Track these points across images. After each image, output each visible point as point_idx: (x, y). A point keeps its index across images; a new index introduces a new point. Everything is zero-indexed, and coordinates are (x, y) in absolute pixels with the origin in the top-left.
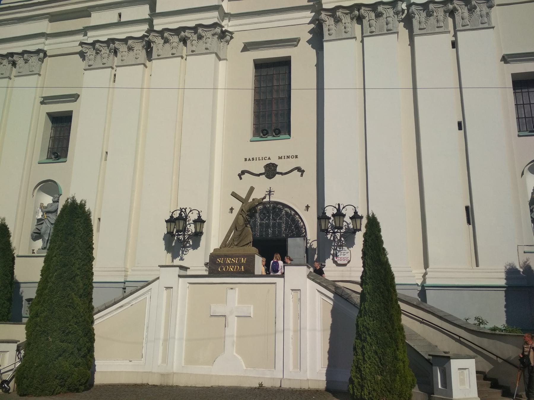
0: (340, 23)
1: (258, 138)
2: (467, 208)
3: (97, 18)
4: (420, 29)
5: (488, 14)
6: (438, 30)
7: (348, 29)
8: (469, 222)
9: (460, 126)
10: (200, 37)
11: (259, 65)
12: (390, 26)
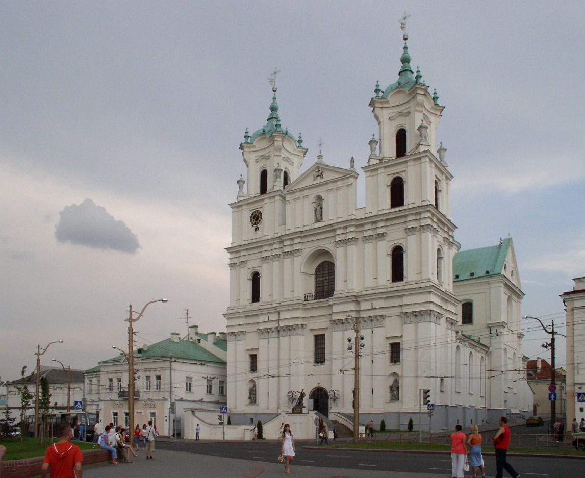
1: (316, 364)
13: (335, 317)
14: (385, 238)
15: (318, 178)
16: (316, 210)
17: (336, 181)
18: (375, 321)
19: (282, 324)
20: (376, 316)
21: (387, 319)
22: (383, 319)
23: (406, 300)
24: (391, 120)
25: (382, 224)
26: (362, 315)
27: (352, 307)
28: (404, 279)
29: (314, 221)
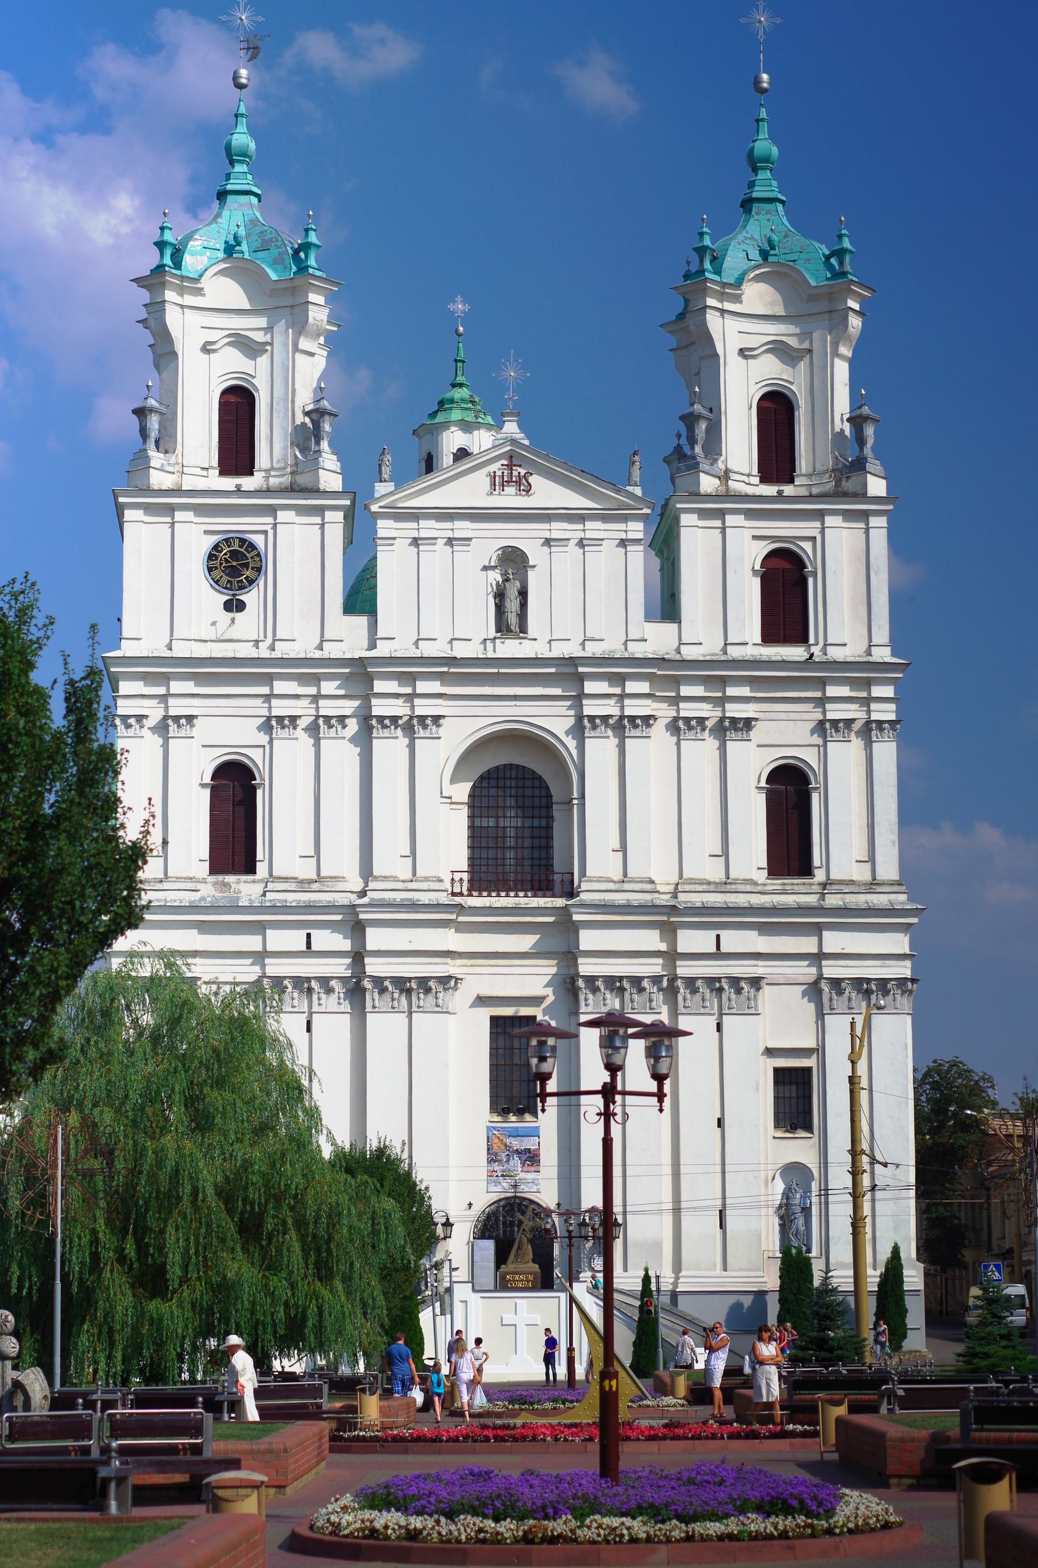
2: (721, 1211)
3: (279, 940)
4: (685, 1007)
6: (702, 1011)
8: (721, 1227)
9: (720, 1123)
10: (428, 990)
12: (654, 1004)
13: (587, 967)
14: (752, 734)
15: (511, 490)
16: (500, 596)
19: (374, 967)
21: (767, 990)
22: (758, 989)
23: (834, 941)
24: (746, 357)
25: (745, 691)
26: (685, 969)
27: (651, 940)
28: (816, 872)
29: (492, 633)
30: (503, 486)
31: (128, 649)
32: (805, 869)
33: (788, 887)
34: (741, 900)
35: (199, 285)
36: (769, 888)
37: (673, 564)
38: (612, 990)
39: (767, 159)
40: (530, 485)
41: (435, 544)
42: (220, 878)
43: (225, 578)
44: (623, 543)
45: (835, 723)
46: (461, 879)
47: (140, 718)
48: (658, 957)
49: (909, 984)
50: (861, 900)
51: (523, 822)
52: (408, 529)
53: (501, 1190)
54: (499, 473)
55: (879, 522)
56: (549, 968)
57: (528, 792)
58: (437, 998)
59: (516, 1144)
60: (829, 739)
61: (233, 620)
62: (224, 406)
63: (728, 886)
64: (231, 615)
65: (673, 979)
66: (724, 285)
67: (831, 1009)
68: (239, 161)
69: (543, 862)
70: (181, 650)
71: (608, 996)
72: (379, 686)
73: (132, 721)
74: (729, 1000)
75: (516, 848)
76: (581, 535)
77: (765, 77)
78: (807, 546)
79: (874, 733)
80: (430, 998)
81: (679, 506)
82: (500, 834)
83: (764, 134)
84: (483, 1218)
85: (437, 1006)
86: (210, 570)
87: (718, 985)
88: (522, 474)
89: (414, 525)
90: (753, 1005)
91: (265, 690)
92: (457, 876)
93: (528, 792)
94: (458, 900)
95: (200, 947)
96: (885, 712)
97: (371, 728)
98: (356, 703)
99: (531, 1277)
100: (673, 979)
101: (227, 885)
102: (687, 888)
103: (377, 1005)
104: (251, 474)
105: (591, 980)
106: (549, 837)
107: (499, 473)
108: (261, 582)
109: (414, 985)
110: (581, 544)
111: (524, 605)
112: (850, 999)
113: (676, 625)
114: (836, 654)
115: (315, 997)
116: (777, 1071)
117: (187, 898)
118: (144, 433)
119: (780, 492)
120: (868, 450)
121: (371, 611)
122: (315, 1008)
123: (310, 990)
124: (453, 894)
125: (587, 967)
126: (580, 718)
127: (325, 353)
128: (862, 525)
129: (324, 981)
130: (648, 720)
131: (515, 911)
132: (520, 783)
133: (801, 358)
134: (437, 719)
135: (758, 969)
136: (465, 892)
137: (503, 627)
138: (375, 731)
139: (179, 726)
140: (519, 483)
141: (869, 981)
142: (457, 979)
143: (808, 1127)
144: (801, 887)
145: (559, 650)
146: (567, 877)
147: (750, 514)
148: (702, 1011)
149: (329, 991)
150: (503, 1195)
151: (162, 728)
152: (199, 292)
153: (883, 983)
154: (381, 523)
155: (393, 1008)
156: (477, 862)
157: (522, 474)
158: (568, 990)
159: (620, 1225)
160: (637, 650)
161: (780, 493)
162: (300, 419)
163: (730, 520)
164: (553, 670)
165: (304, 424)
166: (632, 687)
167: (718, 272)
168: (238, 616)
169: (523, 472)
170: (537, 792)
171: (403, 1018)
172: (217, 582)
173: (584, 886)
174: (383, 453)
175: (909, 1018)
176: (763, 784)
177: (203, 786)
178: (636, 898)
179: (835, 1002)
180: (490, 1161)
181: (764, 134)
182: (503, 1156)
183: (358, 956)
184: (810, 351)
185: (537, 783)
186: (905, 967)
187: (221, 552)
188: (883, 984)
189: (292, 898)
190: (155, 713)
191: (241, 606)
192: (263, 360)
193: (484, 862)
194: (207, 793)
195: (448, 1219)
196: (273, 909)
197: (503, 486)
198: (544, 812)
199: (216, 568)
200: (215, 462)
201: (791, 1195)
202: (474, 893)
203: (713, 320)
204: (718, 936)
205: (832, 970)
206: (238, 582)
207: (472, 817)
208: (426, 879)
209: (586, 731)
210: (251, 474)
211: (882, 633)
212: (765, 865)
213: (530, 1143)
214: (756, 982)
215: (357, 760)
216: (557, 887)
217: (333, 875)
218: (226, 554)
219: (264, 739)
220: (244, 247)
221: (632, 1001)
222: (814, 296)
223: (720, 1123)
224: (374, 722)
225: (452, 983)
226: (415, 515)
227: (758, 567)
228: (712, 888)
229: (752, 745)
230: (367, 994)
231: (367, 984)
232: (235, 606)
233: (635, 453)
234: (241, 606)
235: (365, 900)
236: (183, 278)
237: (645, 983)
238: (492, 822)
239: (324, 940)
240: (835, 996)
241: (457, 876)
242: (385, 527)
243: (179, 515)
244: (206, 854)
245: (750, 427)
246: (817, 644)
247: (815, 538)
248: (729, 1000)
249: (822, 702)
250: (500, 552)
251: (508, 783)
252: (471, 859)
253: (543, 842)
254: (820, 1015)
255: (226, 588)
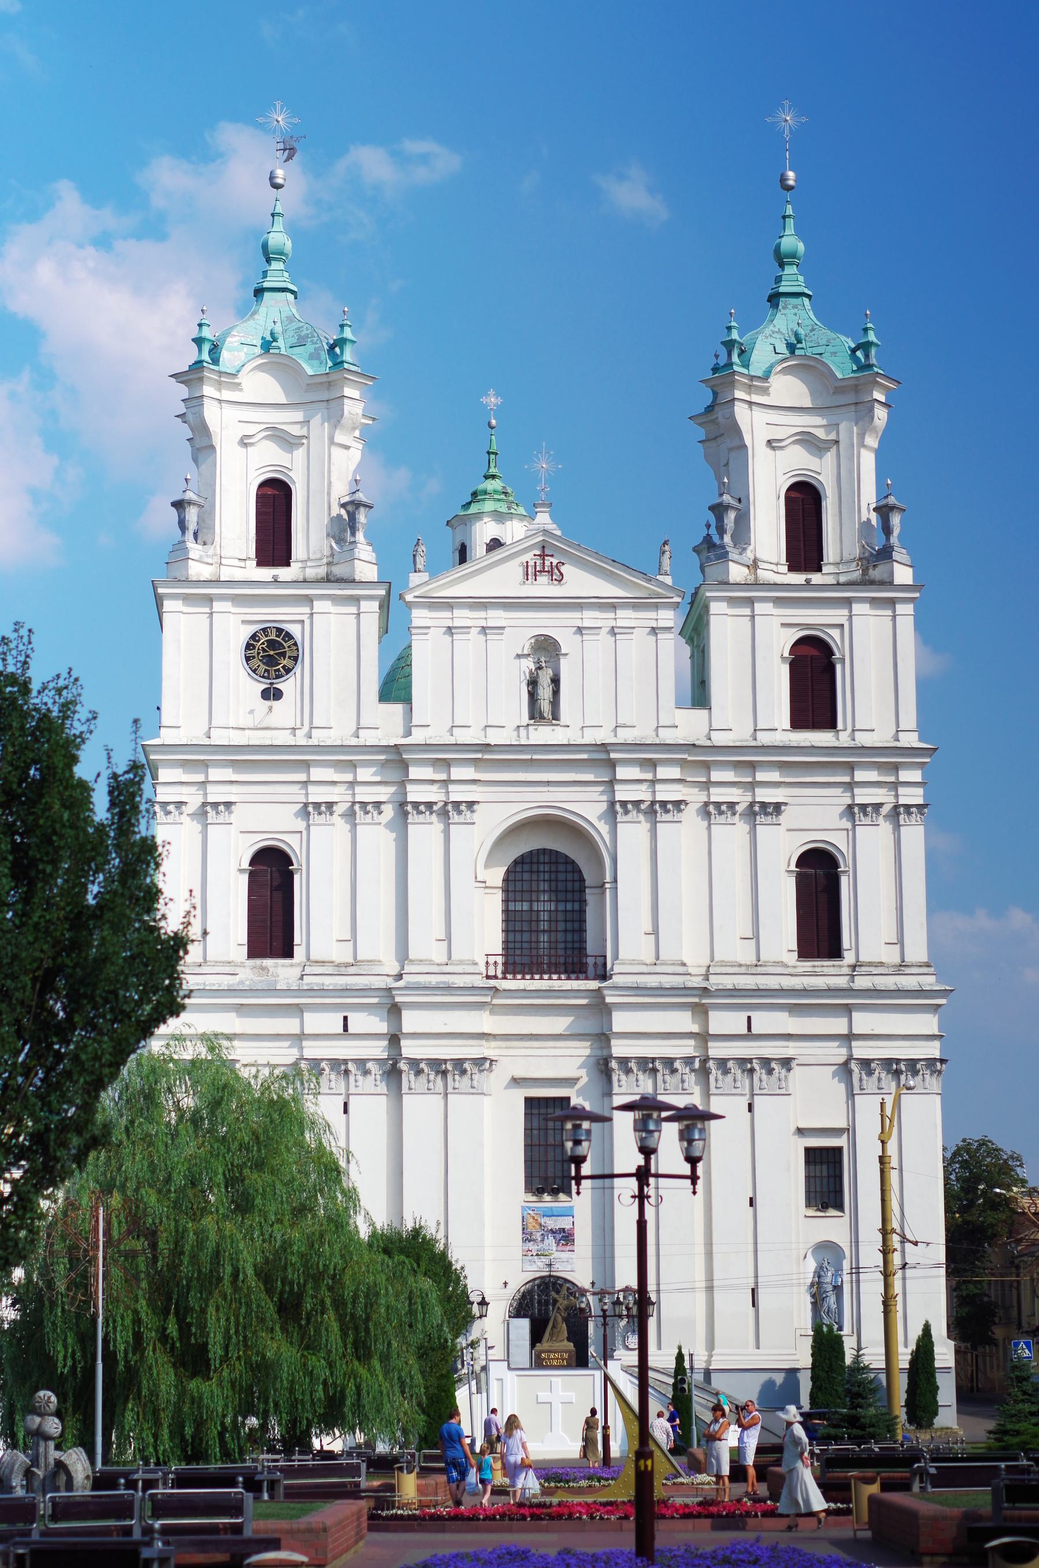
0: (631, 1074)
2: (753, 1290)
4: (717, 1088)
5: (786, 1077)
6: (734, 1091)
7: (639, 1083)
8: (754, 1305)
9: (752, 1202)
10: (464, 1072)
11: (529, 1102)
12: (686, 1085)
13: (620, 1049)
14: (782, 818)
15: (543, 579)
16: (533, 683)
17: (613, 607)
18: (760, 1072)
19: (410, 1049)
20: (766, 1062)
21: (797, 1070)
22: (789, 1070)
23: (864, 1022)
24: (774, 448)
25: (774, 776)
26: (717, 1050)
27: (684, 1021)
28: (846, 954)
29: (525, 719)
30: (535, 575)
31: (167, 737)
32: (835, 952)
33: (817, 969)
34: (772, 983)
35: (236, 381)
36: (800, 970)
37: (703, 651)
38: (645, 1071)
39: (793, 255)
40: (562, 574)
41: (468, 633)
42: (258, 962)
43: (263, 667)
44: (654, 631)
45: (863, 807)
46: (496, 963)
47: (179, 804)
48: (690, 1038)
49: (938, 1064)
50: (889, 982)
51: (556, 906)
52: (443, 618)
53: (537, 1269)
54: (531, 563)
55: (905, 610)
56: (583, 1050)
57: (561, 876)
58: (472, 1080)
59: (551, 1223)
60: (858, 823)
61: (270, 709)
62: (262, 499)
63: (759, 968)
64: (268, 703)
65: (705, 1061)
66: (752, 378)
67: (861, 1089)
68: (275, 259)
69: (577, 945)
70: (219, 738)
71: (641, 1076)
72: (414, 773)
73: (171, 808)
74: (761, 1080)
75: (550, 931)
76: (613, 623)
77: (791, 174)
78: (835, 633)
79: (902, 817)
80: (466, 1079)
81: (708, 594)
82: (534, 918)
83: (790, 229)
84: (518, 1297)
85: (472, 1087)
86: (248, 659)
87: (749, 1066)
88: (554, 564)
89: (448, 614)
90: (783, 1084)
91: (302, 777)
92: (492, 959)
93: (561, 876)
94: (492, 983)
95: (238, 1031)
96: (913, 796)
97: (406, 814)
98: (392, 789)
99: (566, 1356)
100: (705, 1061)
101: (263, 968)
102: (718, 970)
103: (413, 1086)
104: (288, 565)
105: (624, 1061)
106: (582, 921)
107: (531, 563)
108: (298, 669)
109: (449, 1067)
110: (613, 632)
111: (556, 692)
112: (879, 1079)
113: (706, 712)
114: (864, 739)
115: (352, 1078)
116: (808, 1151)
117: (226, 982)
118: (182, 525)
119: (808, 581)
120: (894, 539)
121: (406, 699)
122: (352, 1090)
123: (347, 1072)
124: (488, 977)
125: (620, 1049)
126: (612, 803)
127: (360, 446)
128: (889, 613)
129: (361, 1063)
130: (678, 804)
131: (548, 994)
132: (553, 868)
133: (828, 449)
134: (471, 804)
135: (789, 1049)
136: (500, 975)
137: (535, 714)
138: (410, 816)
139: (217, 813)
140: (551, 572)
141: (898, 1061)
142: (492, 1061)
143: (839, 1206)
144: (831, 969)
145: (592, 737)
146: (600, 960)
147: (778, 602)
148: (734, 1091)
149: (366, 1073)
150: (538, 1275)
151: (201, 814)
152: (237, 386)
153: (912, 1063)
154: (416, 613)
155: (429, 1089)
156: (511, 945)
157: (554, 564)
158: (602, 1072)
159: (654, 1304)
160: (668, 736)
161: (808, 581)
162: (336, 510)
163: (759, 608)
164: (585, 756)
165: (339, 516)
166: (663, 772)
167: (746, 366)
168: (276, 704)
169: (555, 561)
170: (570, 877)
171: (438, 1100)
172: (254, 671)
173: (617, 969)
174: (418, 544)
175: (938, 1099)
176: (793, 867)
177: (241, 871)
178: (668, 981)
179: (864, 1082)
180: (526, 1240)
181: (790, 229)
182: (538, 1236)
183: (394, 1039)
184: (837, 442)
185: (570, 868)
186: (934, 1047)
187: (258, 641)
188: (912, 1065)
189: (329, 982)
190: (193, 799)
191: (278, 695)
192: (300, 453)
193: (518, 945)
194: (245, 879)
195: (483, 1298)
196: (311, 991)
197: (535, 575)
198: (577, 896)
199: (254, 657)
200: (252, 552)
201: (822, 1273)
202: (509, 976)
203: (741, 413)
204: (749, 1018)
205: (862, 1050)
206: (276, 671)
207: (506, 901)
208: (461, 962)
209: (619, 816)
210: (288, 565)
211: (909, 718)
212: (795, 947)
213: (564, 1223)
214: (787, 1063)
215: (393, 845)
216: (591, 970)
217: (369, 958)
218: (263, 643)
219: (301, 825)
220: (281, 343)
221: (665, 1082)
222: (840, 388)
223: (752, 1202)
224: (409, 808)
225: (487, 1064)
226: (448, 604)
227: (786, 654)
228: (743, 970)
229: (781, 829)
230: (404, 1076)
231: (403, 1066)
232: (272, 694)
233: (665, 543)
234: (278, 695)
235: (401, 984)
236: (221, 373)
237: (677, 1065)
238: (526, 906)
239: (359, 1022)
240: (864, 1077)
241: (492, 959)
242: (420, 617)
243: (217, 606)
244: (244, 938)
245: (778, 518)
246: (845, 730)
247: (842, 625)
248: (761, 1080)
249: (850, 786)
250: (533, 641)
251: (541, 868)
252: (506, 942)
253: (576, 925)
254: (851, 1095)
255: (263, 677)
